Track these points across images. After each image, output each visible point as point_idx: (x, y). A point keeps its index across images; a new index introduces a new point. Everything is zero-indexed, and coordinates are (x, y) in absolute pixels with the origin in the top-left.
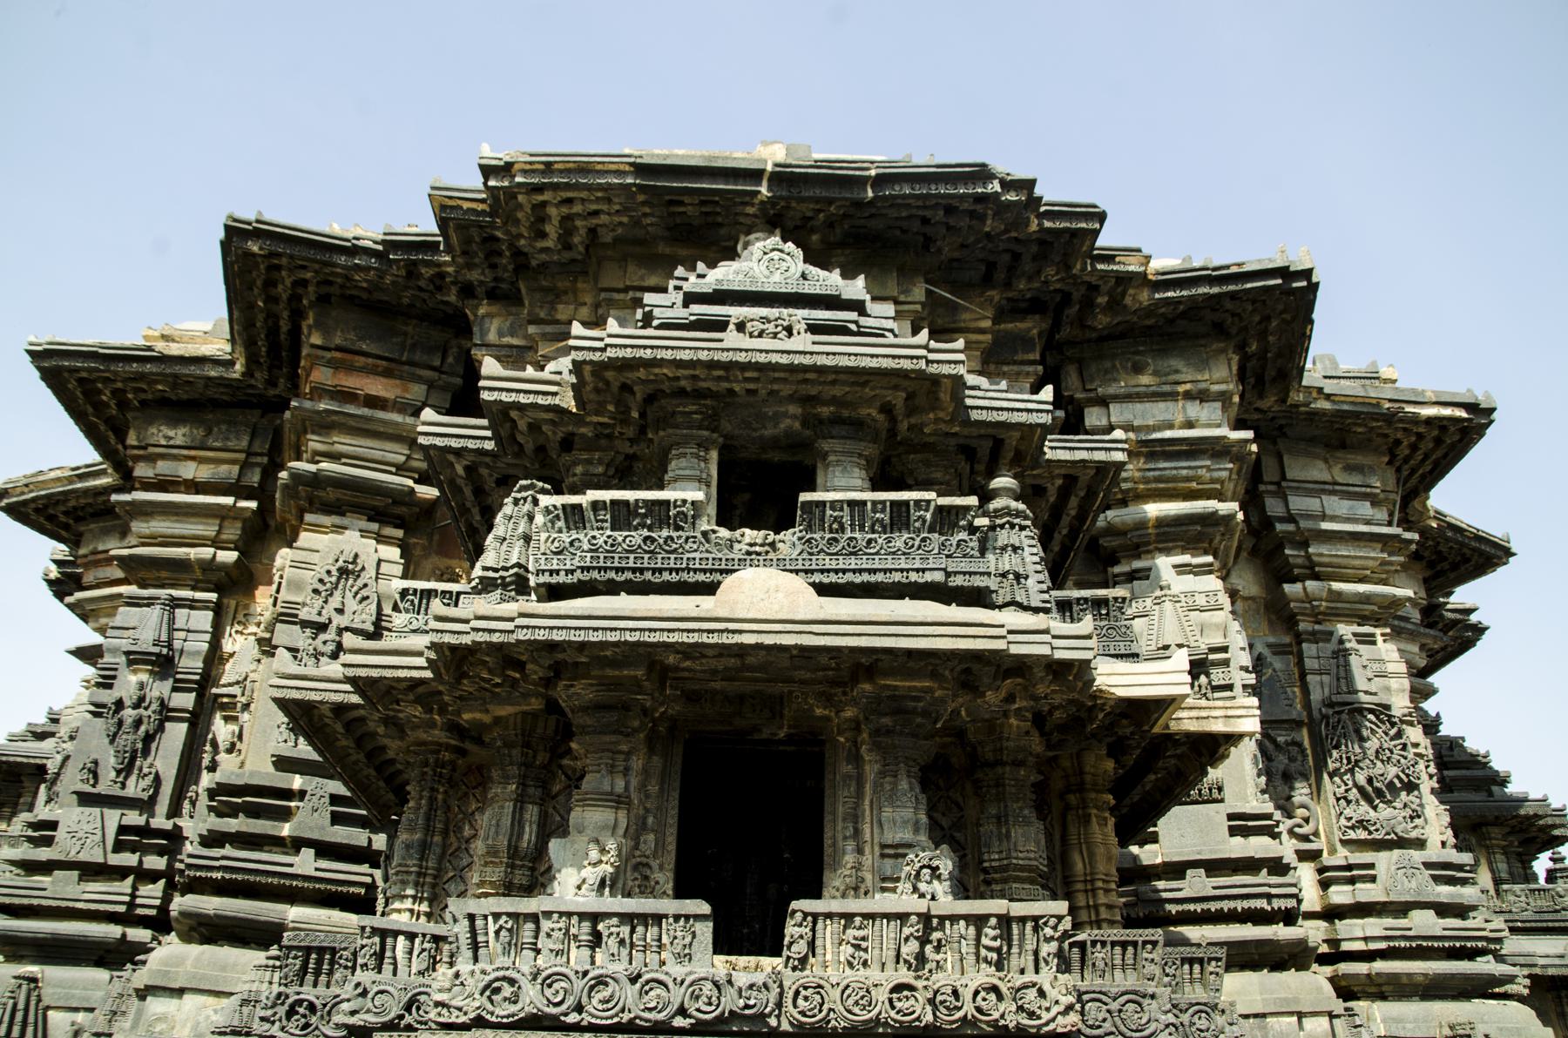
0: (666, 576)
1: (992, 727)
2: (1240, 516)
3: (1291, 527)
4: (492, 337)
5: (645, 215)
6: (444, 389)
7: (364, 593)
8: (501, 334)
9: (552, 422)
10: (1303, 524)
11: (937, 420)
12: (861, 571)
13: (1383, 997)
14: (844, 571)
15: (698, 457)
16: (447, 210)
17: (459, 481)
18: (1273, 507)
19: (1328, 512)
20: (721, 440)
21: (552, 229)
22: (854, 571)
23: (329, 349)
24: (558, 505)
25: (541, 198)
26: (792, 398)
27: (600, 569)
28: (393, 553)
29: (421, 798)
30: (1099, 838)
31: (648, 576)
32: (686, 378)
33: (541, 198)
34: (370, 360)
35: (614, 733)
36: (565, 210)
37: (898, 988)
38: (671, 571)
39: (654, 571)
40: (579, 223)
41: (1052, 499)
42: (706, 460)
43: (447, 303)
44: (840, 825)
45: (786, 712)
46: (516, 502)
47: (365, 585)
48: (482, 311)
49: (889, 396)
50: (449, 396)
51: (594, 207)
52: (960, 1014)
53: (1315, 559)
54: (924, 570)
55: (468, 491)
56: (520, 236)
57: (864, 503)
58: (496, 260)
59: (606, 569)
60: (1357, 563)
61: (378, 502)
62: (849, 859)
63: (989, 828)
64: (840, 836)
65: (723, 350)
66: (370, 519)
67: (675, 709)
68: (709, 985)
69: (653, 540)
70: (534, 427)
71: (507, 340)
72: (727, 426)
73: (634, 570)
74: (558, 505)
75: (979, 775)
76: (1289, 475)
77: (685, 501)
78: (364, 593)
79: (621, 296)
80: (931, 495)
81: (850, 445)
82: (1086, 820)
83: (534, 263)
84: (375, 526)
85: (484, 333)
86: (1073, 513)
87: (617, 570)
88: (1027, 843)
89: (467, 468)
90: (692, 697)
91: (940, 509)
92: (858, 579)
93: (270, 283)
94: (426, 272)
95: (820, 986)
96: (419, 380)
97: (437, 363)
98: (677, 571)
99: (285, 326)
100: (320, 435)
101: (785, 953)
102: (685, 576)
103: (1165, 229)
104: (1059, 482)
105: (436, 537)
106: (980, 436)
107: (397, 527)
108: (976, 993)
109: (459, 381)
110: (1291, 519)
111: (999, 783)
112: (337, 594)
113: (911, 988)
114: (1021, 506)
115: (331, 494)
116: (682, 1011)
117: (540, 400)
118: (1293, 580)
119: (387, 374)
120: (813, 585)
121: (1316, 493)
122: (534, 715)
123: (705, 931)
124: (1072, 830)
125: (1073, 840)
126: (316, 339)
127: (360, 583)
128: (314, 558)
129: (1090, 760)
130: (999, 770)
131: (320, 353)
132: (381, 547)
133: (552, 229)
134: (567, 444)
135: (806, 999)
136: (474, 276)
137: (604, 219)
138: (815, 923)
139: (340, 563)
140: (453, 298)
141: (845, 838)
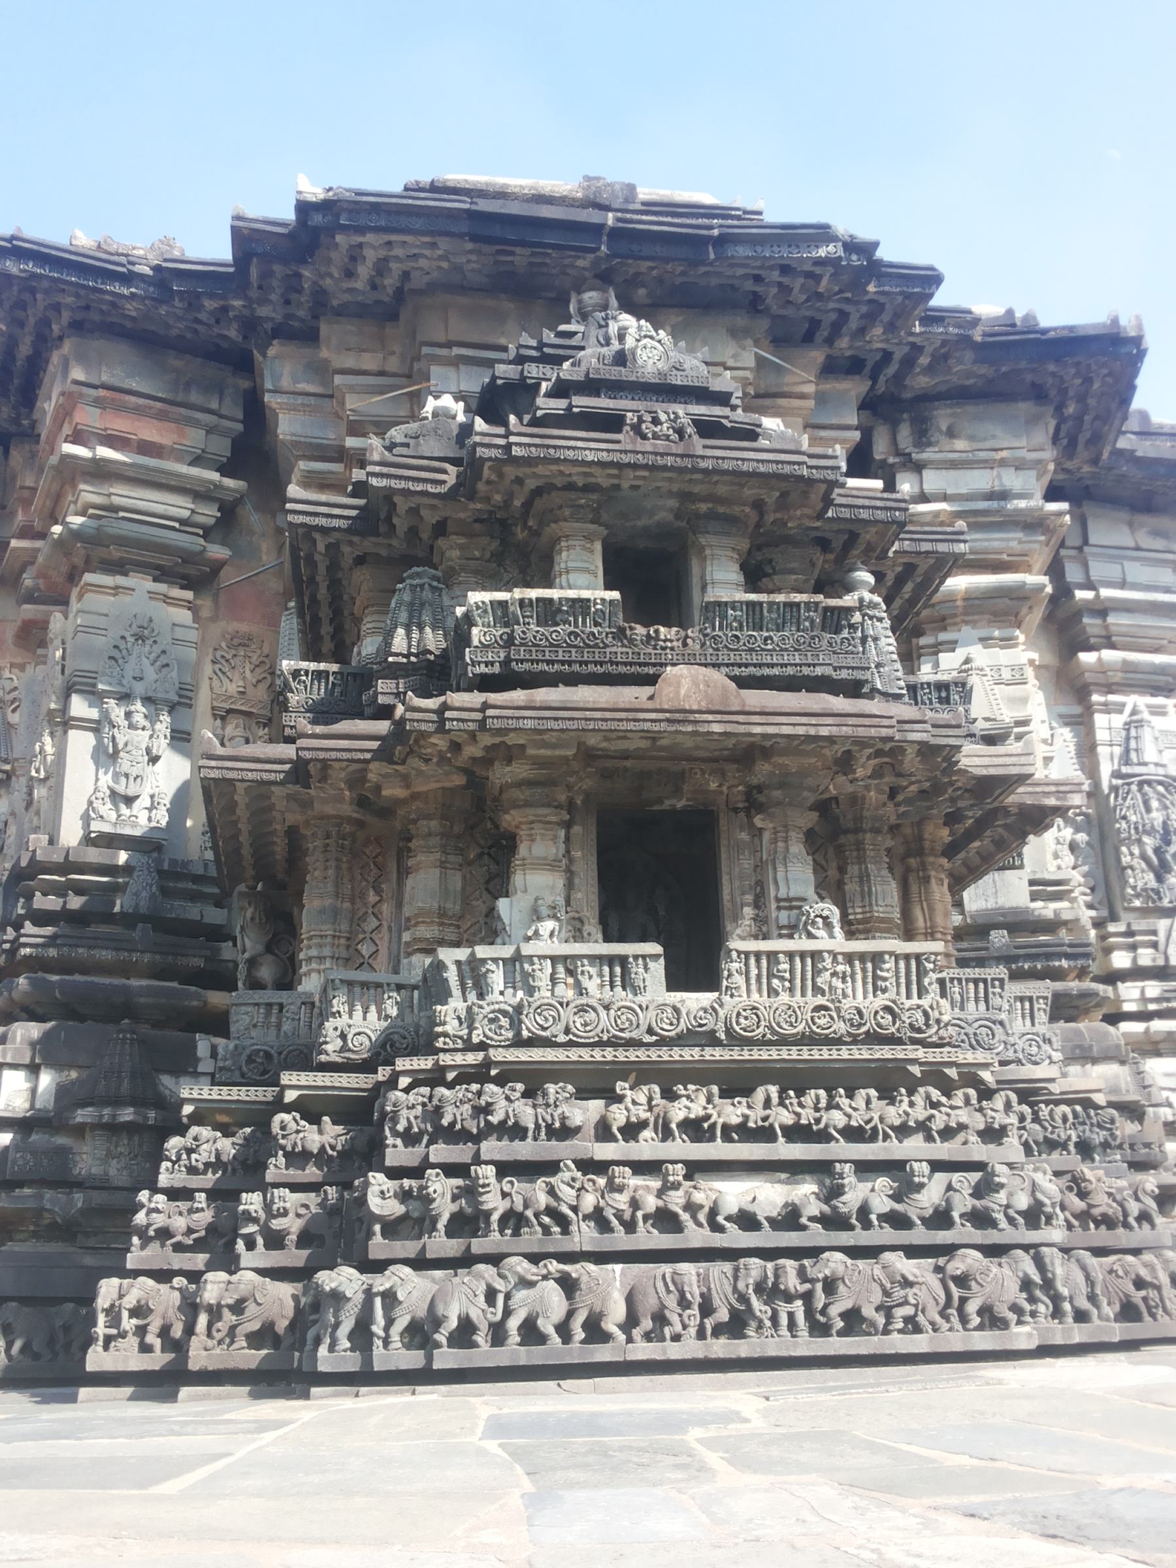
0: (591, 668)
1: (855, 800)
2: (1049, 589)
3: (1088, 595)
4: (286, 383)
5: (469, 261)
6: (223, 433)
7: (163, 660)
8: (296, 381)
9: (433, 507)
10: (1105, 592)
11: (803, 516)
12: (760, 665)
13: (1158, 1054)
14: (746, 666)
15: (584, 548)
16: (247, 238)
17: (317, 557)
18: (1073, 573)
19: (1129, 579)
20: (605, 532)
21: (364, 271)
22: (755, 665)
23: (95, 387)
24: (487, 601)
25: (361, 239)
26: (671, 494)
27: (532, 661)
28: (185, 616)
29: (326, 868)
30: (937, 896)
31: (576, 668)
32: (578, 474)
33: (361, 239)
34: (141, 401)
35: (543, 806)
36: (382, 253)
37: (818, 1008)
38: (596, 663)
39: (581, 663)
40: (393, 265)
41: (889, 584)
42: (592, 552)
43: (224, 337)
44: (737, 883)
45: (685, 787)
46: (413, 588)
47: (164, 652)
48: (271, 352)
49: (763, 493)
50: (228, 442)
51: (416, 251)
52: (864, 1029)
53: (1112, 628)
54: (814, 665)
55: (322, 569)
56: (331, 275)
57: (761, 604)
58: (294, 297)
59: (538, 662)
60: (1154, 633)
61: (164, 560)
62: (748, 911)
63: (851, 887)
64: (737, 892)
65: (621, 451)
66: (155, 580)
67: (588, 784)
68: (669, 1010)
69: (577, 635)
70: (414, 511)
71: (303, 386)
72: (605, 517)
73: (563, 663)
74: (487, 601)
75: (842, 840)
76: (1092, 540)
77: (603, 600)
78: (163, 660)
79: (444, 352)
80: (820, 598)
81: (725, 541)
82: (926, 880)
83: (335, 303)
84: (162, 588)
85: (277, 377)
86: (907, 596)
87: (548, 662)
88: (887, 898)
89: (328, 547)
90: (607, 775)
91: (827, 609)
92: (758, 672)
93: (21, 305)
94: (209, 304)
95: (755, 1008)
96: (196, 423)
97: (214, 405)
98: (601, 664)
99: (25, 349)
100: (92, 484)
101: (725, 983)
102: (611, 668)
103: (986, 283)
104: (899, 569)
105: (222, 597)
106: (838, 531)
107: (183, 587)
108: (876, 1013)
109: (240, 427)
110: (1089, 585)
111: (859, 847)
112: (133, 659)
113: (826, 1008)
114: (877, 599)
115: (115, 553)
116: (650, 1031)
117: (430, 488)
118: (1089, 648)
119: (161, 416)
120: (733, 678)
121: (1118, 559)
122: (452, 790)
123: (658, 968)
124: (914, 888)
125: (915, 897)
126: (78, 374)
127: (157, 649)
128: (101, 622)
129: (929, 830)
130: (860, 836)
131: (85, 390)
132: (172, 609)
133: (364, 271)
134: (441, 529)
135: (746, 1018)
136: (263, 311)
137: (422, 263)
138: (747, 959)
139: (135, 629)
140: (233, 333)
141: (743, 894)
